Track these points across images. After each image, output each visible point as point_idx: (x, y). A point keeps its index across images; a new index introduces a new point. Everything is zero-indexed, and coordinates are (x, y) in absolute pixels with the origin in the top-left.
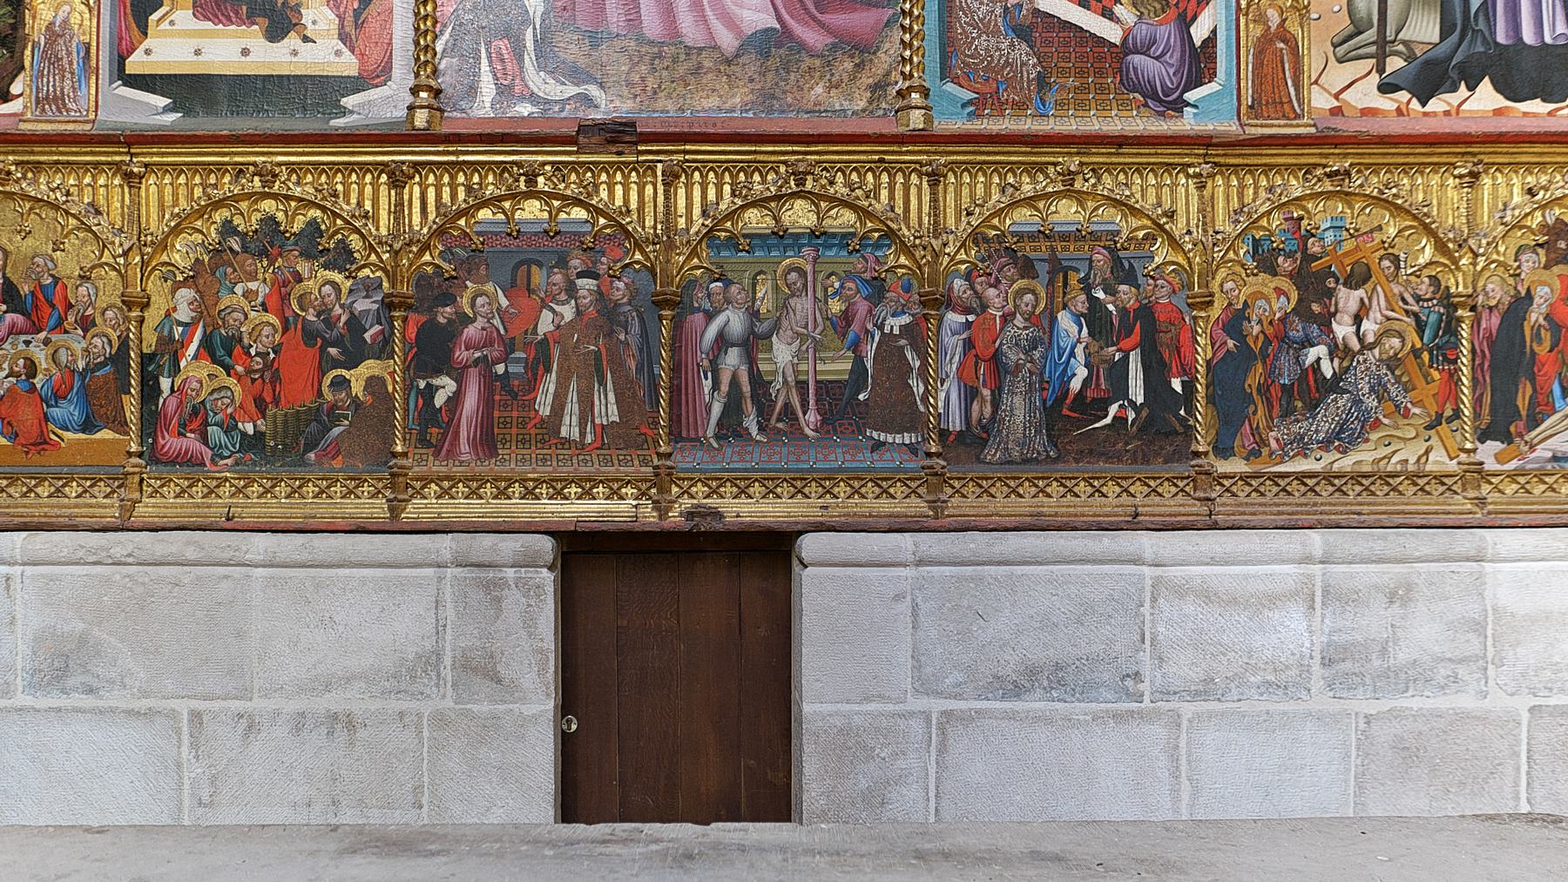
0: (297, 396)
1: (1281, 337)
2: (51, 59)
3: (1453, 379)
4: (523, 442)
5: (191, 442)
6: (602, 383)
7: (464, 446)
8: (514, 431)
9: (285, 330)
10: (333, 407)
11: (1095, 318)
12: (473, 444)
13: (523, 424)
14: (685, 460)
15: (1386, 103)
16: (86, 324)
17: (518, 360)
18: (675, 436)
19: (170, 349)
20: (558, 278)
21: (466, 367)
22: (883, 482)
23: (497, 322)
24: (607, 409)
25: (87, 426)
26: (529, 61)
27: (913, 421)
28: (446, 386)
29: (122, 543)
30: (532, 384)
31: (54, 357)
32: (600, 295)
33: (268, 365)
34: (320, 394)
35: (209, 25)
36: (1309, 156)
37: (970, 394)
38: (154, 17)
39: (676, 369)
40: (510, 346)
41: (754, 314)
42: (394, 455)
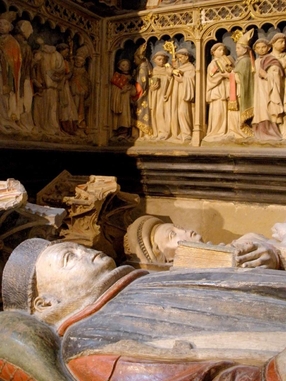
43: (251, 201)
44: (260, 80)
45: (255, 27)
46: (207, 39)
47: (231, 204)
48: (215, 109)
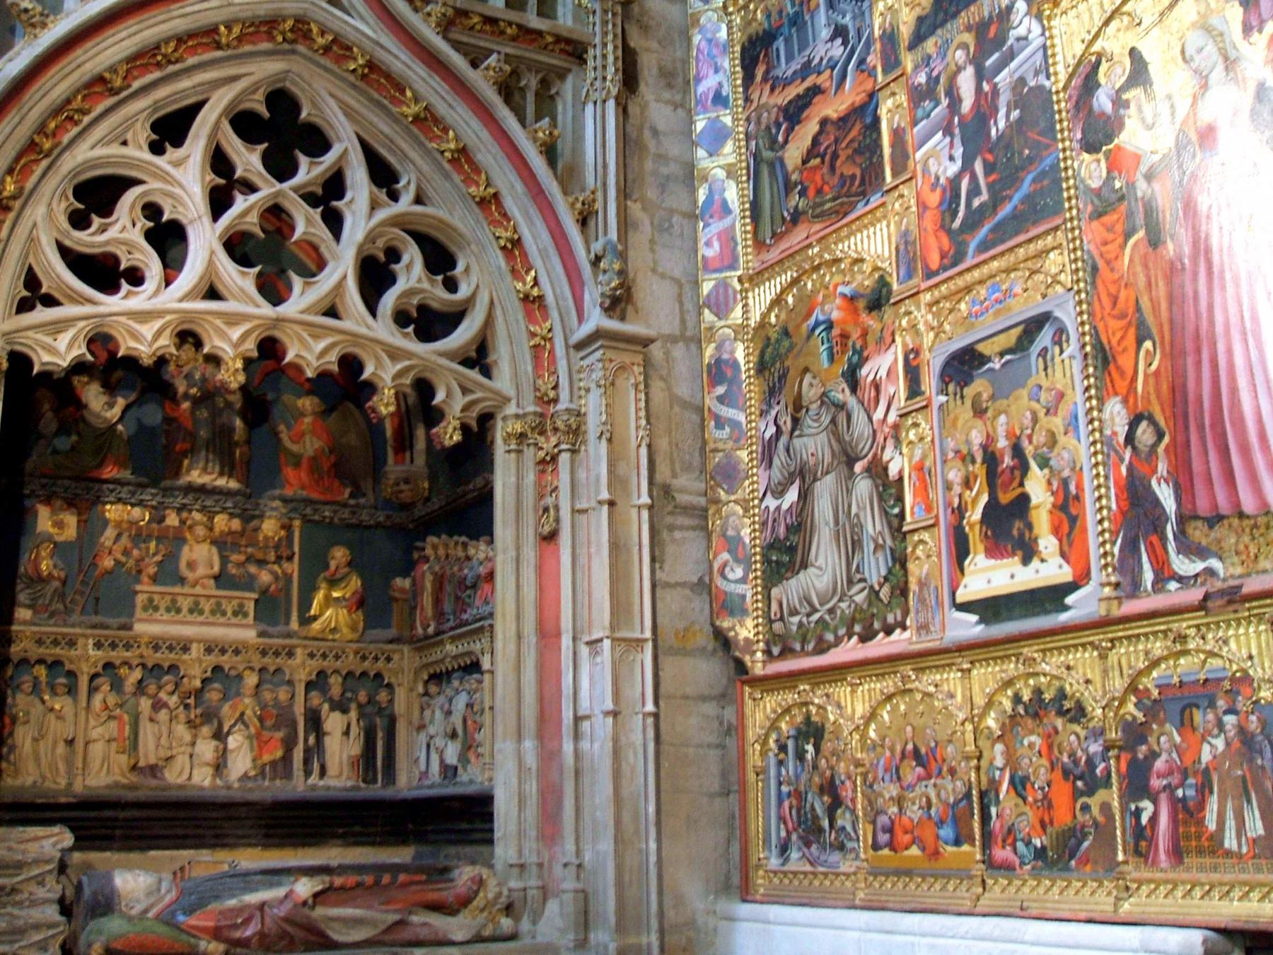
0: (1062, 817)
2: (922, 600)
4: (1200, 852)
6: (1249, 801)
7: (1162, 856)
8: (1194, 843)
9: (1053, 769)
10: (1083, 826)
12: (1167, 853)
13: (1199, 838)
17: (1190, 786)
20: (1210, 716)
21: (1158, 793)
23: (1175, 755)
24: (1255, 826)
25: (957, 842)
26: (1171, 546)
28: (1147, 807)
30: (1201, 805)
31: (938, 795)
32: (1242, 730)
33: (1045, 796)
34: (1075, 816)
35: (992, 562)
38: (967, 562)
40: (1185, 774)
42: (1118, 864)
43: (130, 849)
44: (149, 725)
45: (144, 666)
46: (93, 671)
47: (108, 854)
48: (97, 749)
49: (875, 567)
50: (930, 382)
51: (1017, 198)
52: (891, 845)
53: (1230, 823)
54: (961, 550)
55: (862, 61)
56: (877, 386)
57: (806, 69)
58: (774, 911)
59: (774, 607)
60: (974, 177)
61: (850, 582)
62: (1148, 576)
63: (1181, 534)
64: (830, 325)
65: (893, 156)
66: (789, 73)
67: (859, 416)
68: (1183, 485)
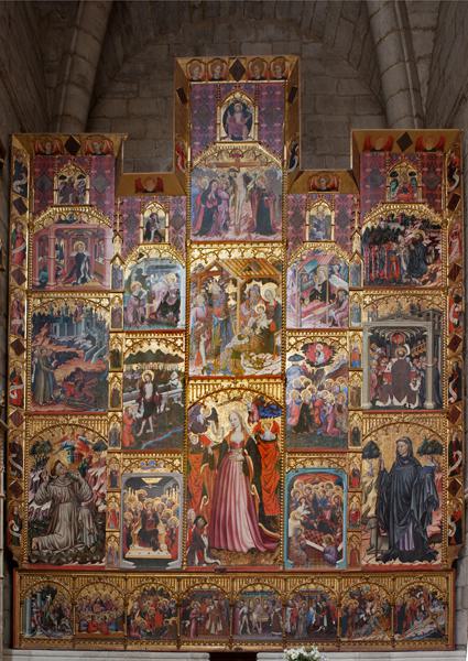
0: (158, 624)
1: (355, 612)
3: (390, 621)
5: (137, 634)
11: (317, 609)
14: (235, 638)
15: (377, 563)
16: (116, 609)
18: (233, 633)
19: (133, 614)
22: (274, 643)
24: (220, 628)
27: (279, 630)
28: (188, 622)
29: (126, 654)
30: (205, 623)
32: (219, 605)
36: (362, 575)
37: (292, 625)
39: (234, 619)
41: (249, 608)
49: (89, 540)
50: (121, 484)
51: (165, 436)
52: (87, 631)
53: (213, 627)
54: (128, 541)
55: (100, 356)
56: (96, 478)
57: (70, 344)
58: (34, 652)
59: (34, 544)
60: (148, 423)
61: (76, 543)
62: (197, 561)
63: (208, 551)
64: (73, 449)
65: (112, 399)
66: (62, 340)
67: (85, 487)
68: (211, 537)
